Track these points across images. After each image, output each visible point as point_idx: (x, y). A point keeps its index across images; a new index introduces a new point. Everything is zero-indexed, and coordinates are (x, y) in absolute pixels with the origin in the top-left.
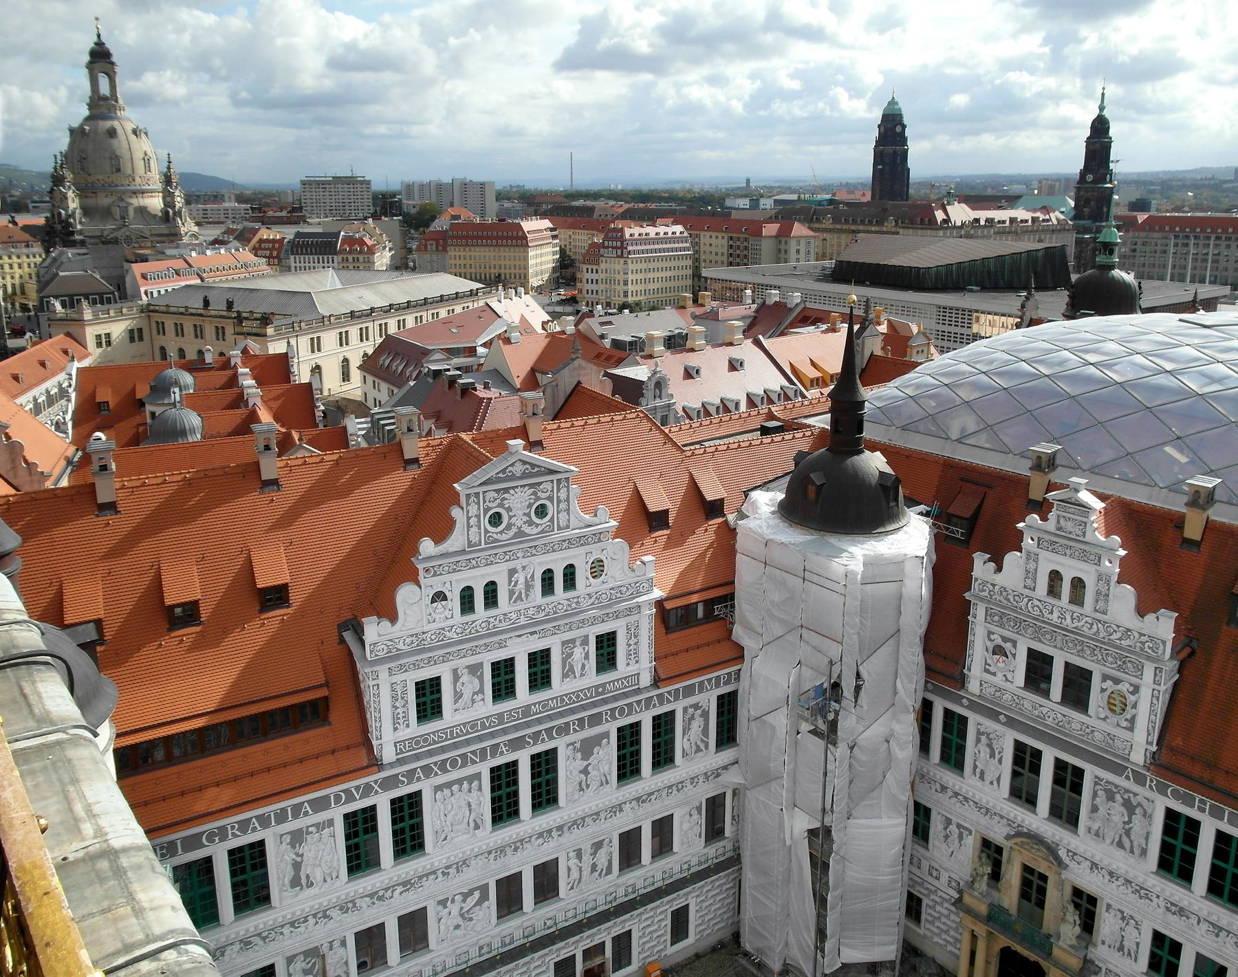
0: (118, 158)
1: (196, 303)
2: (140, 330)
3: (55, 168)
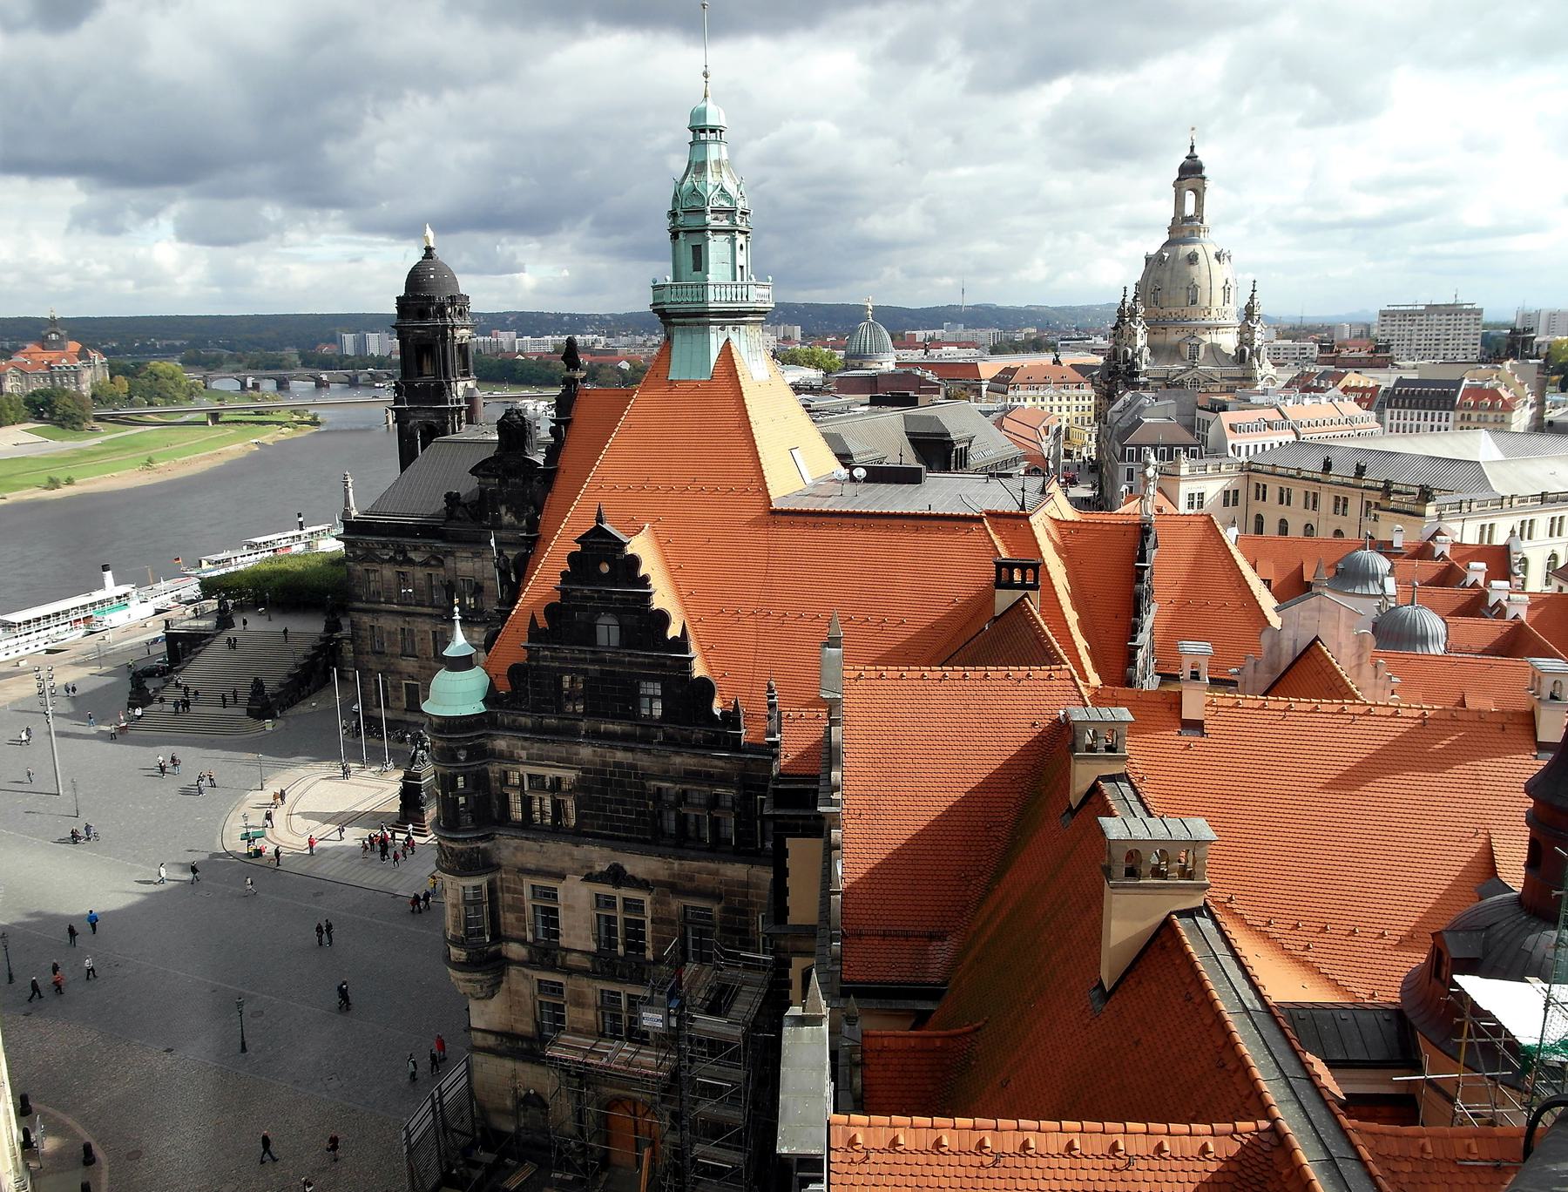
0: (1196, 287)
1: (1313, 465)
2: (1236, 492)
3: (1123, 302)
